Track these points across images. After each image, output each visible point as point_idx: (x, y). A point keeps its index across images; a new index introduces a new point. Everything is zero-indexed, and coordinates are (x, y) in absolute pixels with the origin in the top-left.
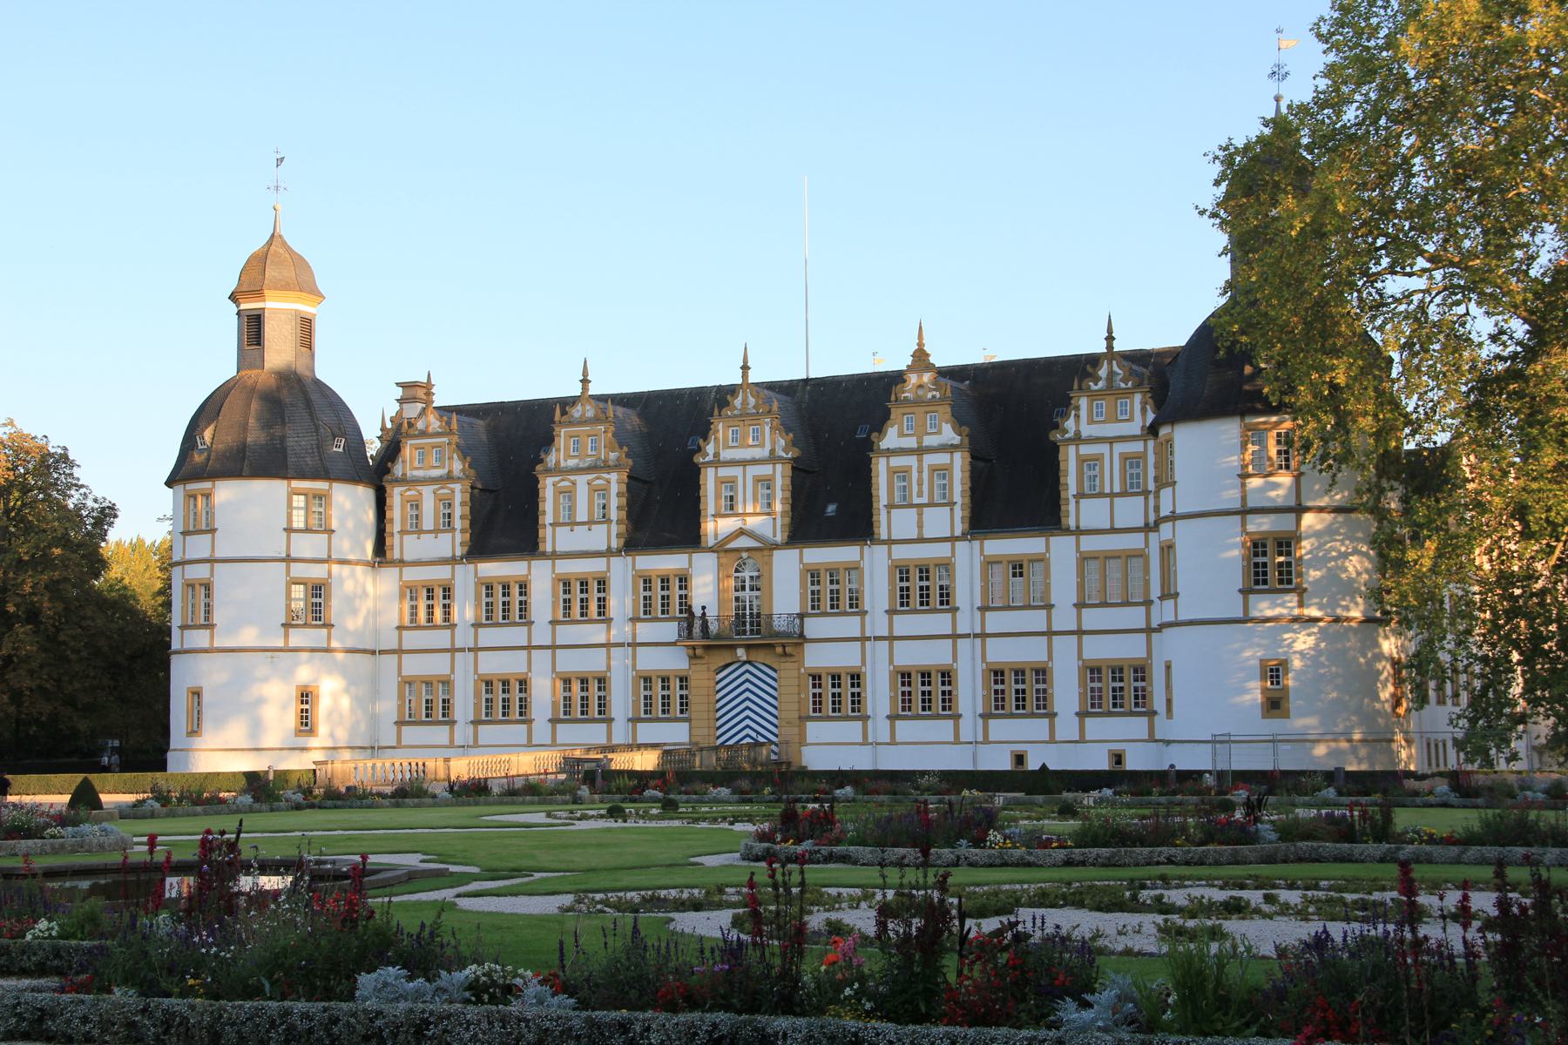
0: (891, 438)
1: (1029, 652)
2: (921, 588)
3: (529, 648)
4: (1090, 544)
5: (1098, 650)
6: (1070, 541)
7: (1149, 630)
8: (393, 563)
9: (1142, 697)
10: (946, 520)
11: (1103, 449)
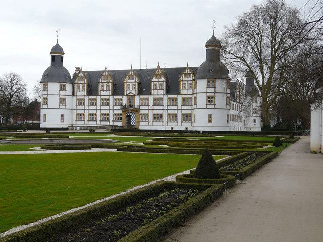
0: (154, 79)
1: (174, 112)
2: (158, 102)
3: (97, 109)
4: (184, 96)
5: (184, 112)
6: (181, 96)
7: (192, 110)
8: (75, 96)
9: (191, 119)
11: (186, 82)
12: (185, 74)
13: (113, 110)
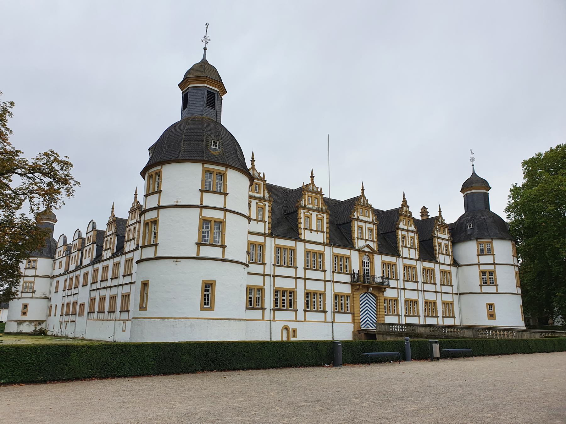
10: (414, 254)
12: (440, 226)
13: (334, 282)
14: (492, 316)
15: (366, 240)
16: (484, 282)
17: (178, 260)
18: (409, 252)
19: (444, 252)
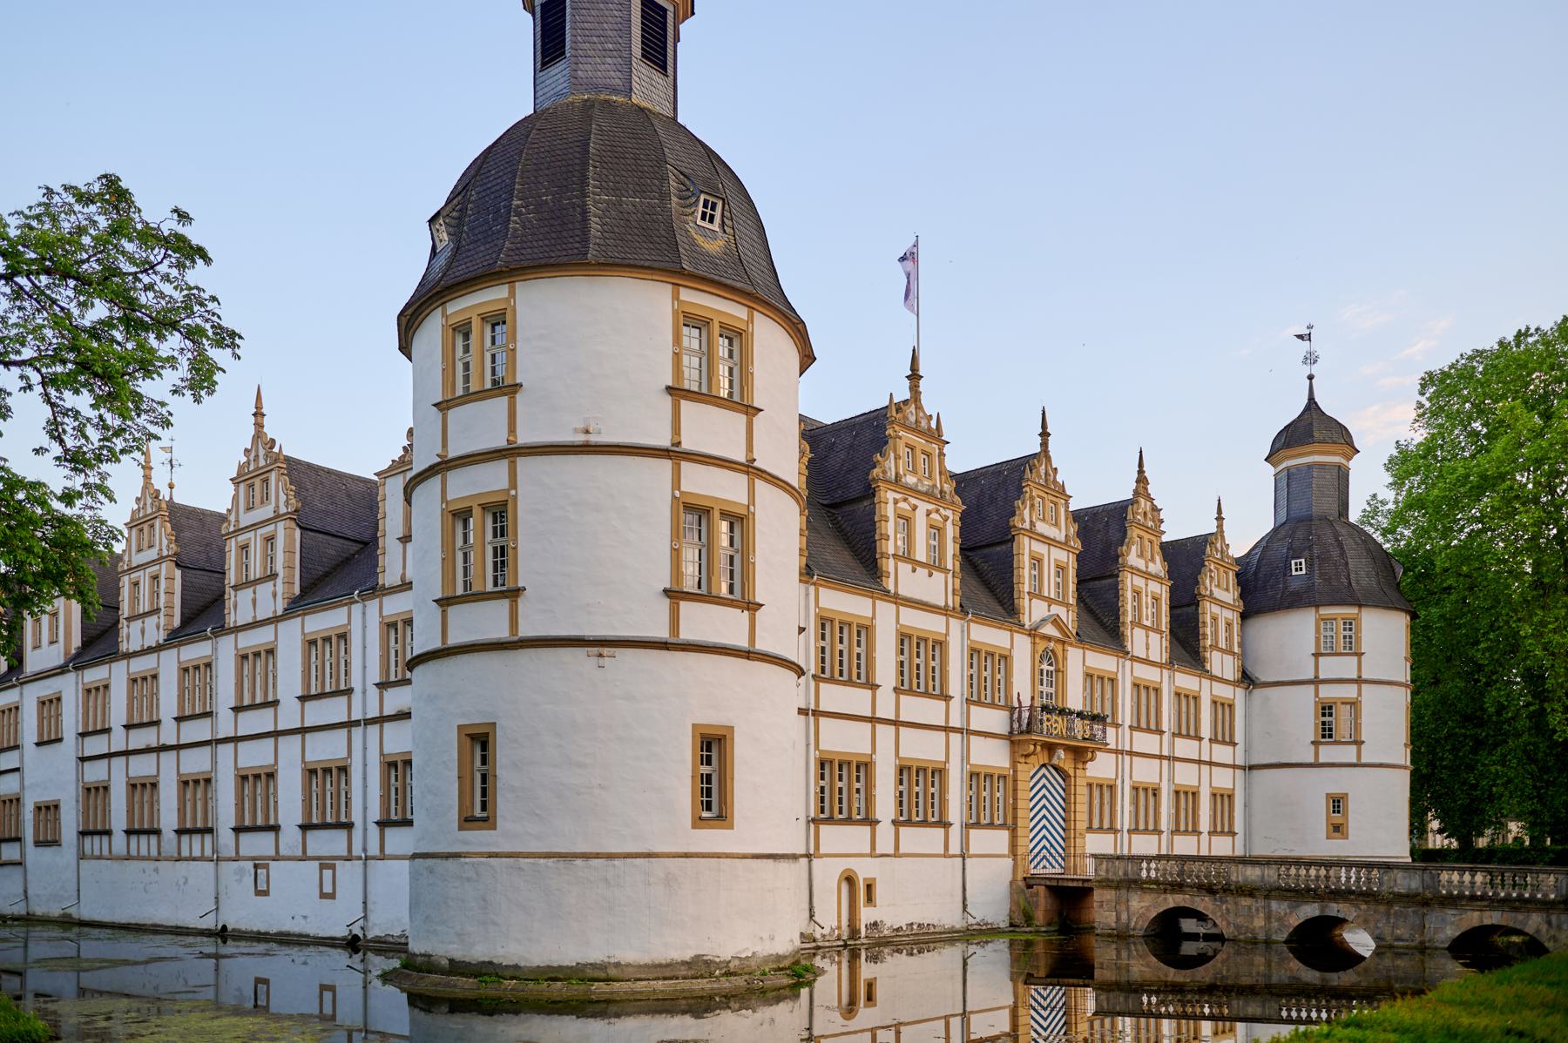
14: (1337, 829)
15: (1050, 601)
16: (1327, 733)
17: (606, 651)
18: (1148, 641)
19: (1222, 644)
